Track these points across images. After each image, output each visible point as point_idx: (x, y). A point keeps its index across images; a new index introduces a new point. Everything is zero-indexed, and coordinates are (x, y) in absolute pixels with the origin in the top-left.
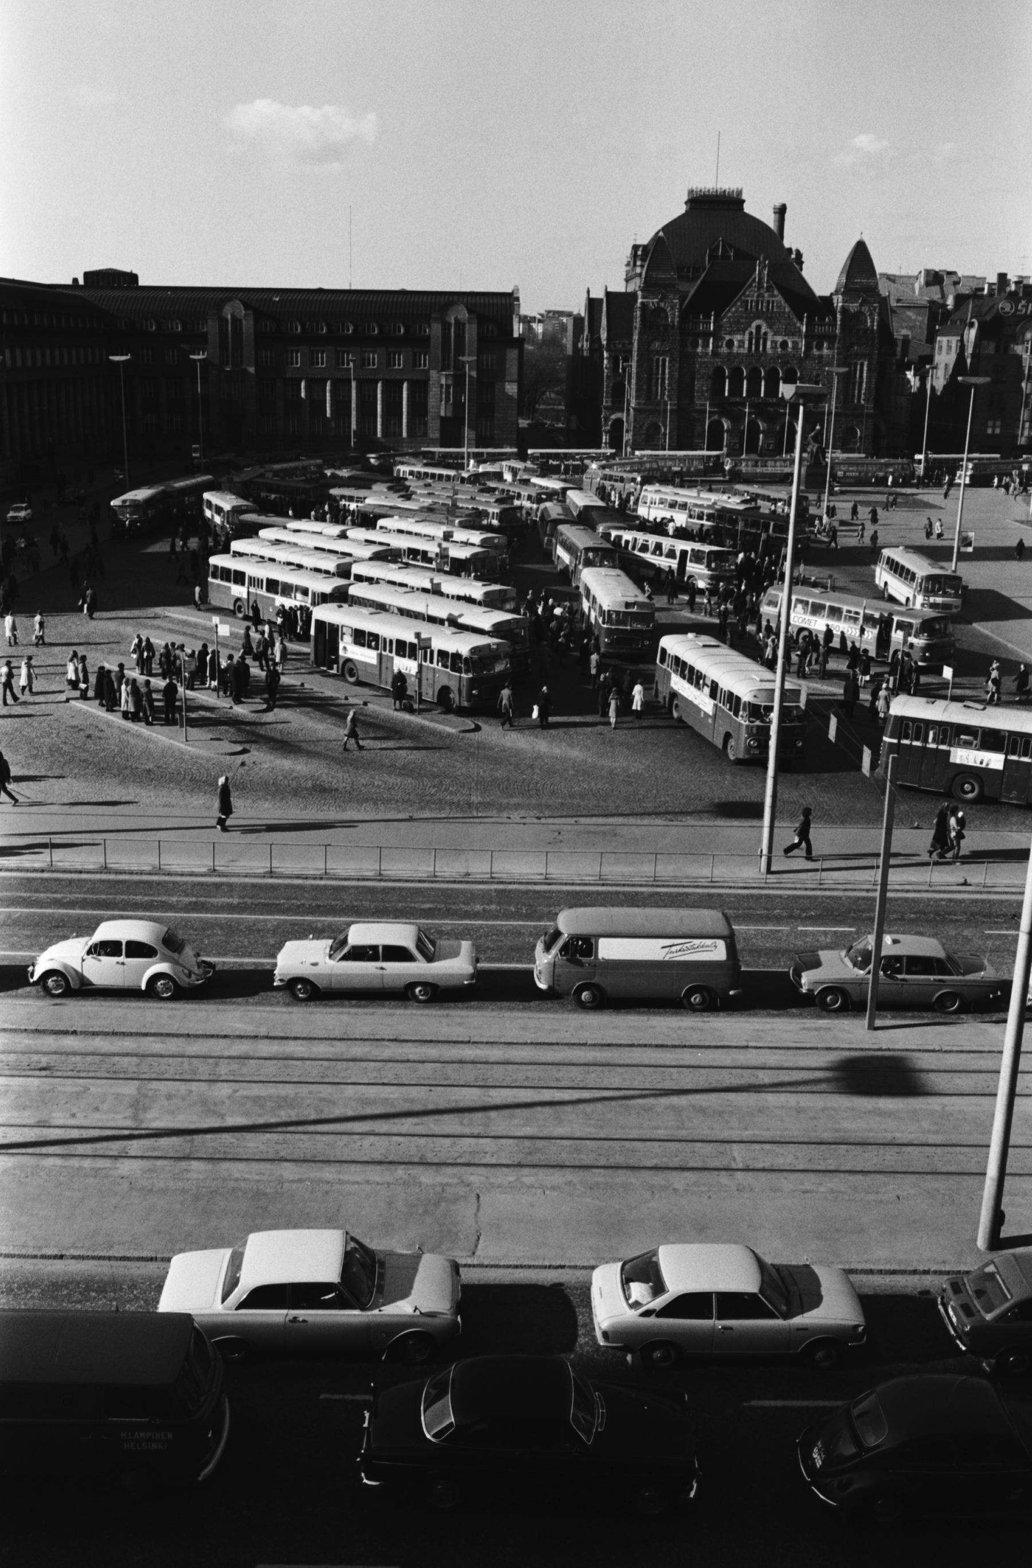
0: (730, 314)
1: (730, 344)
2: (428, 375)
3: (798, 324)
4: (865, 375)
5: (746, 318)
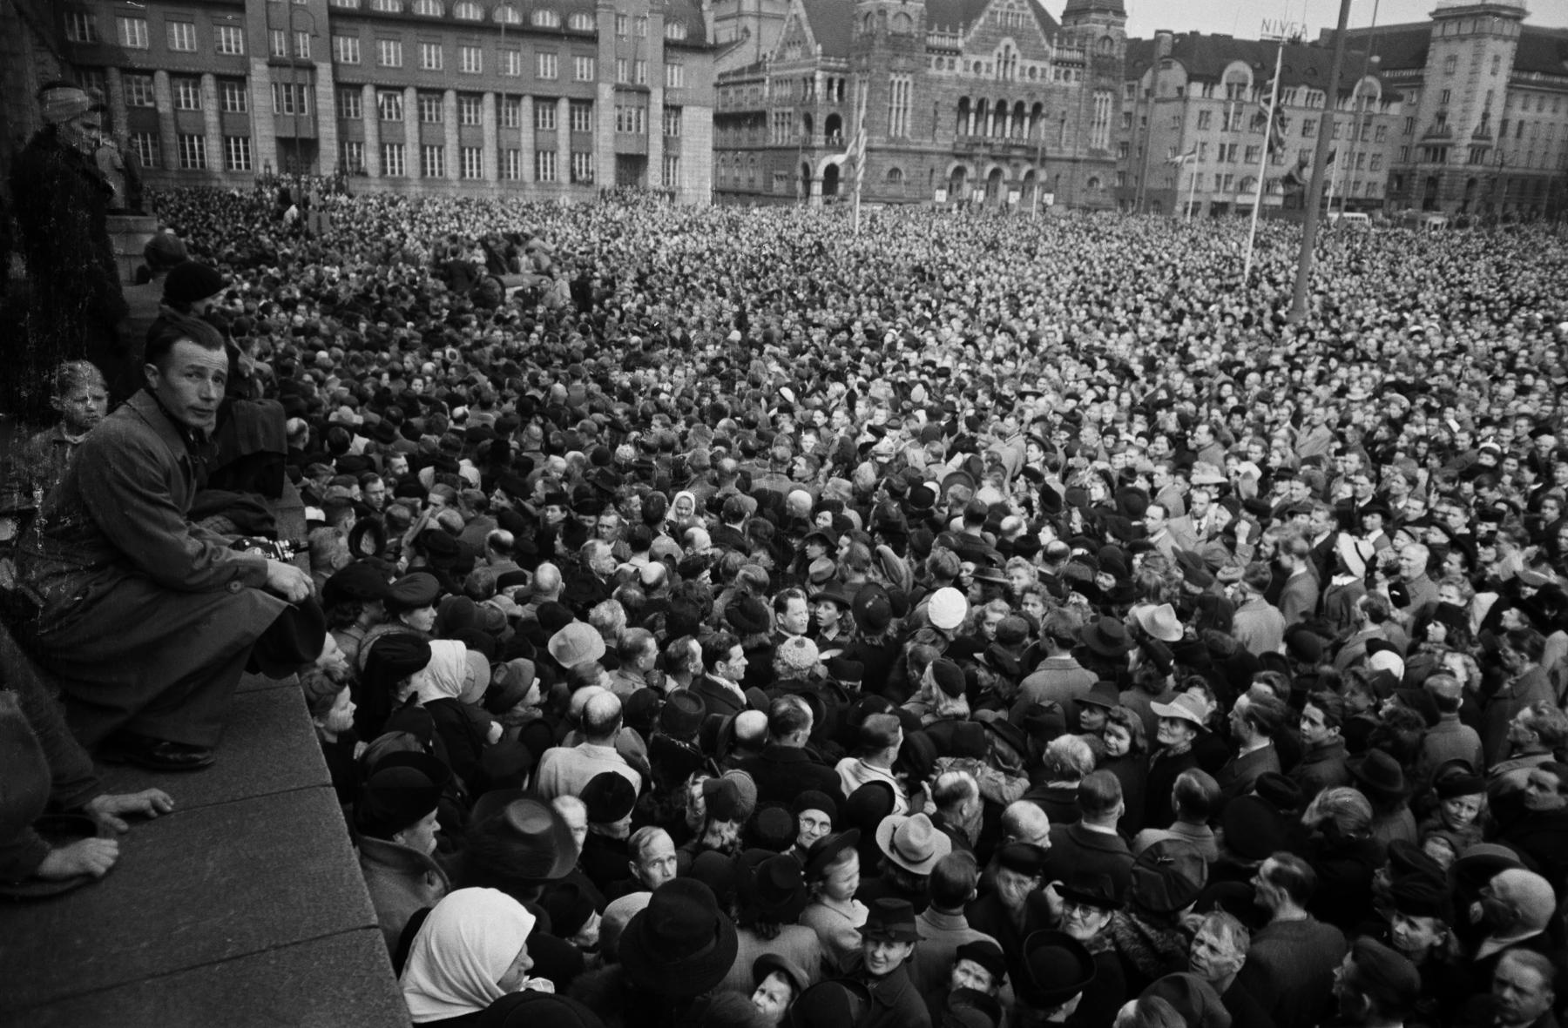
1: (977, 65)
2: (595, 93)
3: (1047, 47)
4: (1109, 114)
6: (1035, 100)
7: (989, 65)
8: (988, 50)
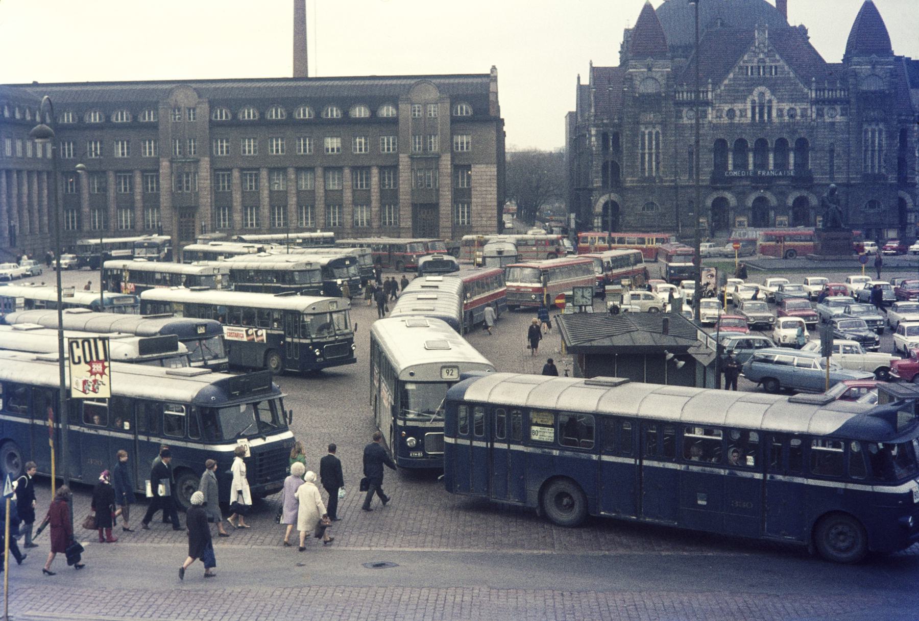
0: (726, 82)
2: (398, 161)
3: (806, 90)
4: (884, 142)
5: (746, 85)
6: (797, 136)
7: (743, 112)
8: (744, 99)
